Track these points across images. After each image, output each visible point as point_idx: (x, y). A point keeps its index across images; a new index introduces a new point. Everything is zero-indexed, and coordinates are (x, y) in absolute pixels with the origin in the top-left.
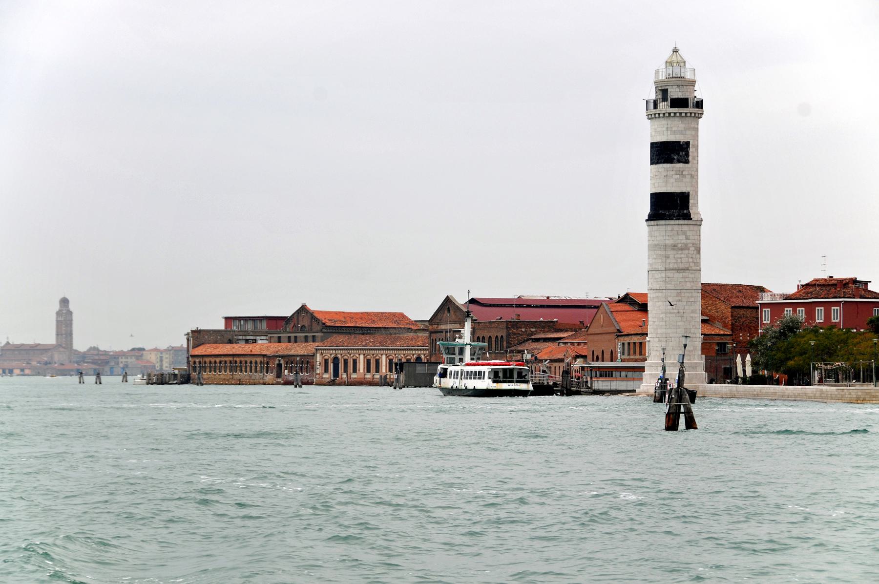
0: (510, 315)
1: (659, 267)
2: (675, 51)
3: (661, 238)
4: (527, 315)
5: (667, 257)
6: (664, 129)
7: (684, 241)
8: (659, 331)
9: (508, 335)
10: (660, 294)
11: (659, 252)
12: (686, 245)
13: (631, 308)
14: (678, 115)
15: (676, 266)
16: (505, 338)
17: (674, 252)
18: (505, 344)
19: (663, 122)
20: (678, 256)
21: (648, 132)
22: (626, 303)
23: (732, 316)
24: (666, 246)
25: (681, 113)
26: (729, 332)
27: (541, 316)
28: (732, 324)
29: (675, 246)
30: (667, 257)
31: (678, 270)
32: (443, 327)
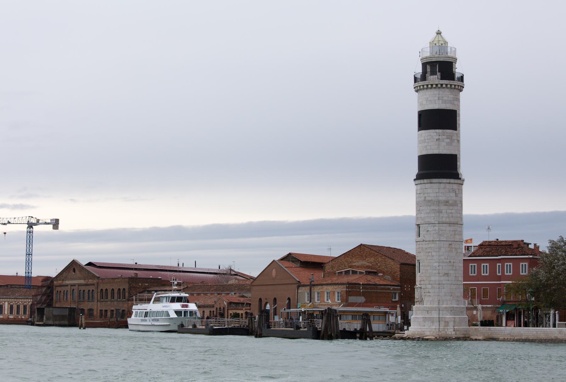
0: (132, 273)
1: (433, 221)
2: (439, 33)
3: (435, 195)
4: (141, 274)
5: (440, 212)
6: (436, 98)
7: (454, 198)
8: (433, 278)
9: (130, 288)
10: (433, 245)
11: (433, 207)
12: (455, 201)
13: (294, 265)
14: (449, 86)
15: (447, 220)
16: (127, 290)
18: (127, 294)
19: (435, 92)
20: (449, 211)
21: (412, 103)
22: (289, 261)
23: (400, 271)
24: (439, 202)
25: (451, 85)
26: (398, 283)
27: (151, 275)
28: (401, 278)
29: (447, 202)
30: (440, 212)
31: (450, 224)
32: (67, 282)
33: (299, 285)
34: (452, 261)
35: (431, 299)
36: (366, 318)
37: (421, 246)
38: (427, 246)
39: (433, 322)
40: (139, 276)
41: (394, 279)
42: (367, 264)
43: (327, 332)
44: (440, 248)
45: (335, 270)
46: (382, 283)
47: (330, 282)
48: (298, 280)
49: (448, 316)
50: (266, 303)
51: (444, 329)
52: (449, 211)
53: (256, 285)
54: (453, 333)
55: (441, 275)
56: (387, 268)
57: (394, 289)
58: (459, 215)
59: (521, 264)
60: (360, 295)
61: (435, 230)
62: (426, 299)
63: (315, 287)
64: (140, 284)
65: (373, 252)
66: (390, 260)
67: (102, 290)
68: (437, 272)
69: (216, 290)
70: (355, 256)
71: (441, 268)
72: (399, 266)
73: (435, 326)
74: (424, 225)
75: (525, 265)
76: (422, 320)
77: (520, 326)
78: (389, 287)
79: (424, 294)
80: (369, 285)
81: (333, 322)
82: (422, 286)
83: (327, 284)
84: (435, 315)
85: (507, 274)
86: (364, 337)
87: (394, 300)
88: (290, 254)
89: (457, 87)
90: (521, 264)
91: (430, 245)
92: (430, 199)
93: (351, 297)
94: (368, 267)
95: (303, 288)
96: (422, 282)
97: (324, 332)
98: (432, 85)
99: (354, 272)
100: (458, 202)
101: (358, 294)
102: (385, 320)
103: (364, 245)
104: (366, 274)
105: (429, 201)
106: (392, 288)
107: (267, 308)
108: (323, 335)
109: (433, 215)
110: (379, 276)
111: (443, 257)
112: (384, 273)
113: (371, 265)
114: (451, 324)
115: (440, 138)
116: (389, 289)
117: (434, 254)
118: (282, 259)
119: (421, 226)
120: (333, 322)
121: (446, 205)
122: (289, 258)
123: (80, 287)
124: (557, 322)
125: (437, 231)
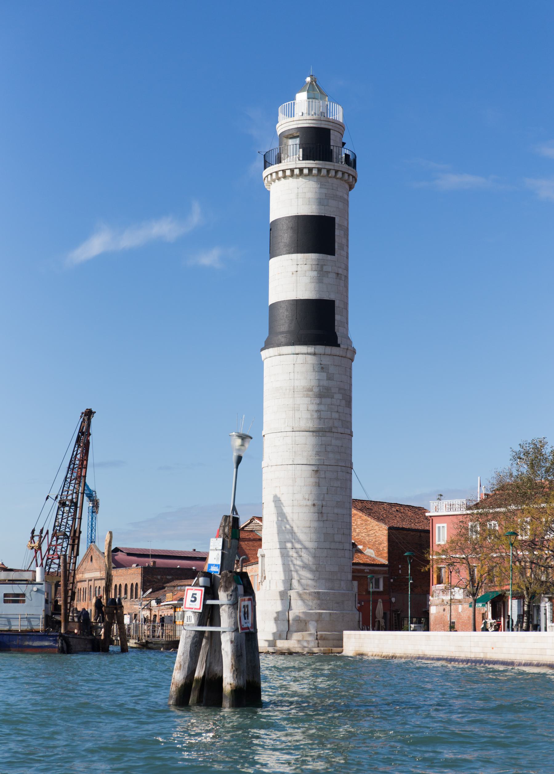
16: (139, 585)
27: (179, 564)
40: (157, 566)
56: (368, 535)
64: (159, 577)
67: (116, 586)
77: (513, 630)
89: (332, 173)
98: (284, 171)
115: (299, 269)
123: (96, 582)
124: (549, 624)
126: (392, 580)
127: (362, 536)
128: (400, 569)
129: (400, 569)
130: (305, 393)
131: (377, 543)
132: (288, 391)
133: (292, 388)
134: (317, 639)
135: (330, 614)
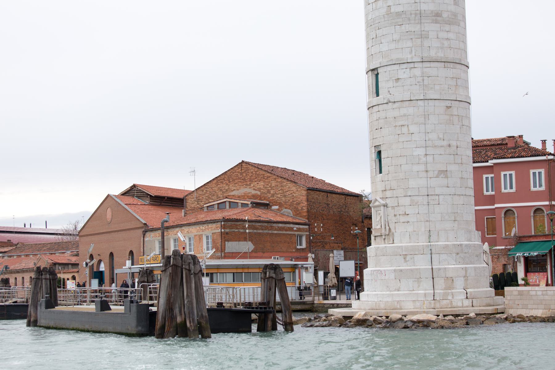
1: (408, 57)
5: (423, 36)
8: (412, 183)
10: (411, 111)
13: (140, 202)
15: (441, 55)
17: (436, 27)
20: (443, 35)
22: (133, 196)
23: (307, 200)
24: (420, 16)
26: (304, 220)
28: (308, 212)
30: (423, 36)
33: (146, 229)
34: (454, 143)
35: (410, 229)
36: (273, 277)
37: (382, 114)
38: (396, 113)
39: (418, 280)
41: (297, 213)
42: (254, 192)
43: (173, 318)
44: (426, 116)
45: (202, 204)
46: (279, 219)
47: (193, 220)
48: (144, 222)
49: (452, 266)
50: (100, 261)
51: (446, 294)
52: (443, 35)
53: (87, 235)
54: (467, 303)
55: (430, 174)
56: (285, 196)
57: (299, 230)
58: (462, 45)
59: (532, 172)
60: (245, 240)
61: (415, 76)
62: (399, 230)
63: (170, 231)
65: (262, 172)
66: (290, 185)
68: (422, 167)
69: (49, 249)
70: (234, 180)
71: (430, 159)
72: (304, 193)
73: (424, 289)
74: (389, 68)
75: (540, 173)
76: (392, 276)
78: (292, 226)
79: (394, 220)
80: (259, 221)
81: (189, 287)
82: (388, 201)
83: (189, 225)
84: (422, 264)
85: (506, 191)
86: (270, 323)
87: (299, 247)
88: (134, 186)
90: (532, 172)
91: (403, 111)
92: (400, 9)
93: (230, 243)
94: (254, 196)
95: (152, 234)
96: (388, 194)
97: (164, 318)
99: (233, 205)
100: (460, 17)
101: (243, 237)
102: (294, 280)
103: (247, 163)
104: (253, 207)
105: (398, 14)
106: (295, 227)
107: (101, 270)
108: (163, 327)
109: (409, 44)
110: (273, 210)
111: (433, 136)
112: (280, 205)
113: (259, 193)
114: (459, 283)
116: (291, 229)
117: (413, 128)
118: (125, 194)
119: (380, 70)
120: (189, 287)
121: (436, 22)
122: (134, 192)
125: (420, 79)
126: (311, 238)
127: (277, 197)
128: (316, 227)
129: (316, 227)
130: (434, 18)
131: (295, 203)
132: (413, 16)
133: (418, 12)
134: (467, 298)
135: (475, 268)
